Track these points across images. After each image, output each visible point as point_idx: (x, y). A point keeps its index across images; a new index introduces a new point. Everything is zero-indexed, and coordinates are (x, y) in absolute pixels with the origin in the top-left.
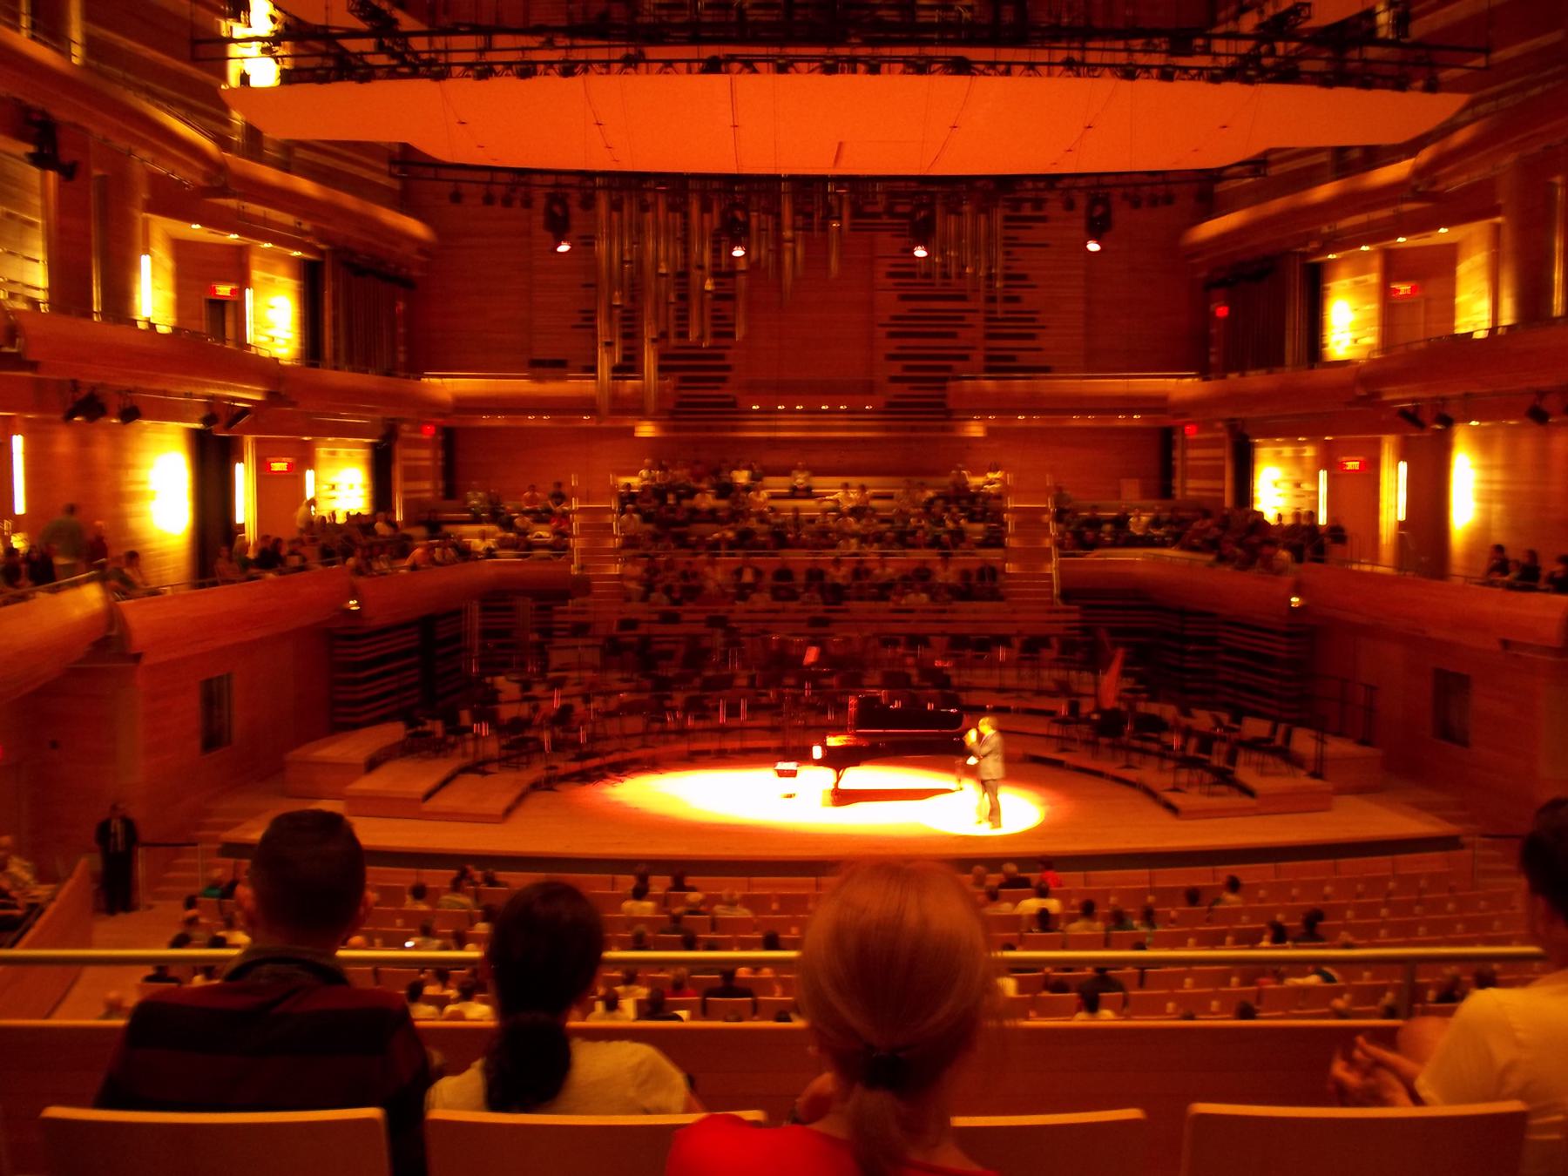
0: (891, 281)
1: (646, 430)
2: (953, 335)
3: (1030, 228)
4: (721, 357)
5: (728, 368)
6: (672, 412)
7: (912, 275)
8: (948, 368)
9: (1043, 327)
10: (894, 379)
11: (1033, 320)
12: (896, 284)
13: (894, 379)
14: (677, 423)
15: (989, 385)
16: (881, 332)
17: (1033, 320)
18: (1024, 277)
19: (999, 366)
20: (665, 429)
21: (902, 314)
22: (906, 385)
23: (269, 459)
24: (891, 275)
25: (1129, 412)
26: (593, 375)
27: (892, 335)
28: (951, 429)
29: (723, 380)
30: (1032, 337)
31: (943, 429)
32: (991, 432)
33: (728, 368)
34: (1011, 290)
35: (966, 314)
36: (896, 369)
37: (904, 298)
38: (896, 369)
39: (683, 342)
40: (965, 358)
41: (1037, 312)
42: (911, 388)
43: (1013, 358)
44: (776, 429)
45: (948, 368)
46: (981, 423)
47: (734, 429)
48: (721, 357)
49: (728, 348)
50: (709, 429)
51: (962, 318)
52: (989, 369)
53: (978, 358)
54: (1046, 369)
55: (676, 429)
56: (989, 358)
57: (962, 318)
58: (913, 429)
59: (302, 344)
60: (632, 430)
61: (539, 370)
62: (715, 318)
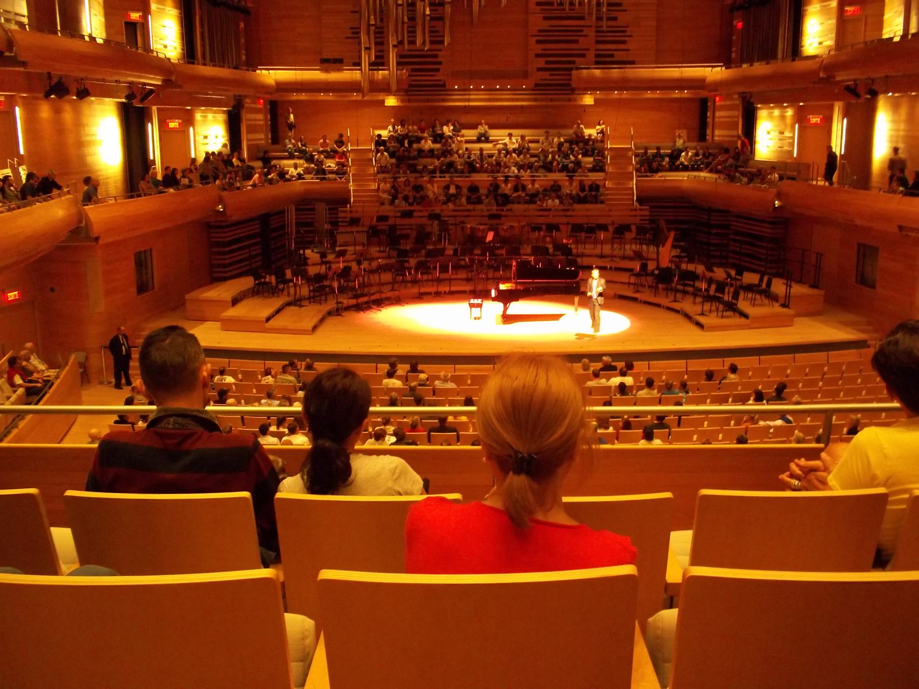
0: (539, 7)
1: (391, 101)
2: (576, 42)
4: (436, 56)
5: (440, 63)
6: (406, 90)
8: (573, 62)
10: (539, 69)
11: (625, 32)
12: (542, 10)
13: (539, 69)
15: (597, 72)
17: (625, 32)
18: (619, 5)
19: (603, 61)
20: (402, 101)
21: (545, 28)
22: (548, 73)
23: (167, 121)
25: (681, 88)
26: (359, 68)
27: (538, 42)
28: (575, 100)
29: (438, 70)
30: (624, 42)
31: (570, 100)
32: (596, 100)
33: (440, 63)
34: (612, 13)
35: (537, 34)
36: (541, 62)
37: (545, 18)
38: (541, 62)
39: (412, 47)
40: (583, 56)
41: (627, 27)
42: (550, 75)
43: (612, 56)
44: (469, 100)
45: (573, 62)
46: (593, 96)
47: (444, 100)
48: (436, 56)
49: (440, 50)
50: (428, 101)
52: (597, 63)
53: (591, 55)
54: (633, 63)
55: (409, 101)
56: (597, 56)
57: (582, 31)
58: (551, 100)
59: (183, 50)
60: (383, 101)
61: (326, 65)
62: (431, 32)
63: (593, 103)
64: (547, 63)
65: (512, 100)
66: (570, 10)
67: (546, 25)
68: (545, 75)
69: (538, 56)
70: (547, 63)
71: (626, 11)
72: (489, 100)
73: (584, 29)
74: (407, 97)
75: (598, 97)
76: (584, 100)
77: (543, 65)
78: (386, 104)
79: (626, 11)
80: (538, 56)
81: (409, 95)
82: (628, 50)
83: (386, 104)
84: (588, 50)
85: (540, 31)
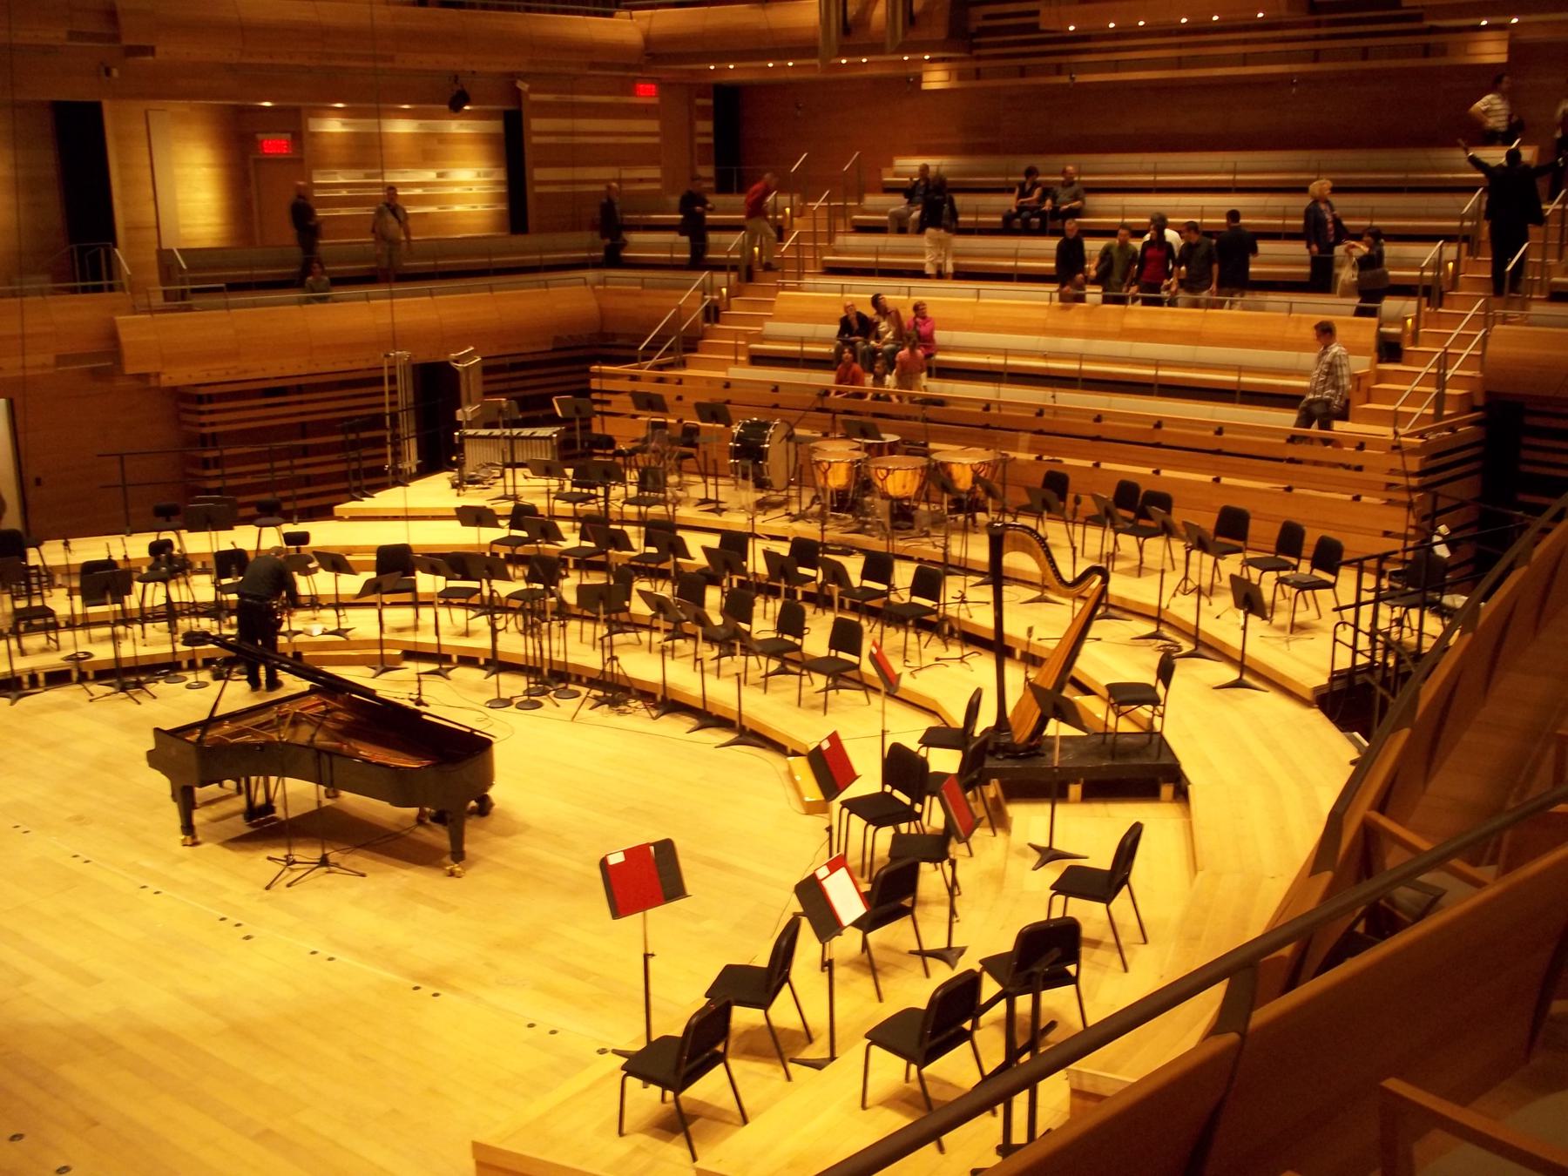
1: (936, 79)
14: (982, 64)
28: (1443, 51)
31: (1427, 51)
32: (1515, 49)
44: (1117, 66)
46: (1505, 35)
55: (978, 74)
58: (1365, 54)
60: (919, 79)
63: (1503, 59)
65: (1245, 60)
72: (1179, 63)
75: (1526, 36)
76: (1473, 49)
78: (925, 86)
81: (979, 58)
83: (925, 86)
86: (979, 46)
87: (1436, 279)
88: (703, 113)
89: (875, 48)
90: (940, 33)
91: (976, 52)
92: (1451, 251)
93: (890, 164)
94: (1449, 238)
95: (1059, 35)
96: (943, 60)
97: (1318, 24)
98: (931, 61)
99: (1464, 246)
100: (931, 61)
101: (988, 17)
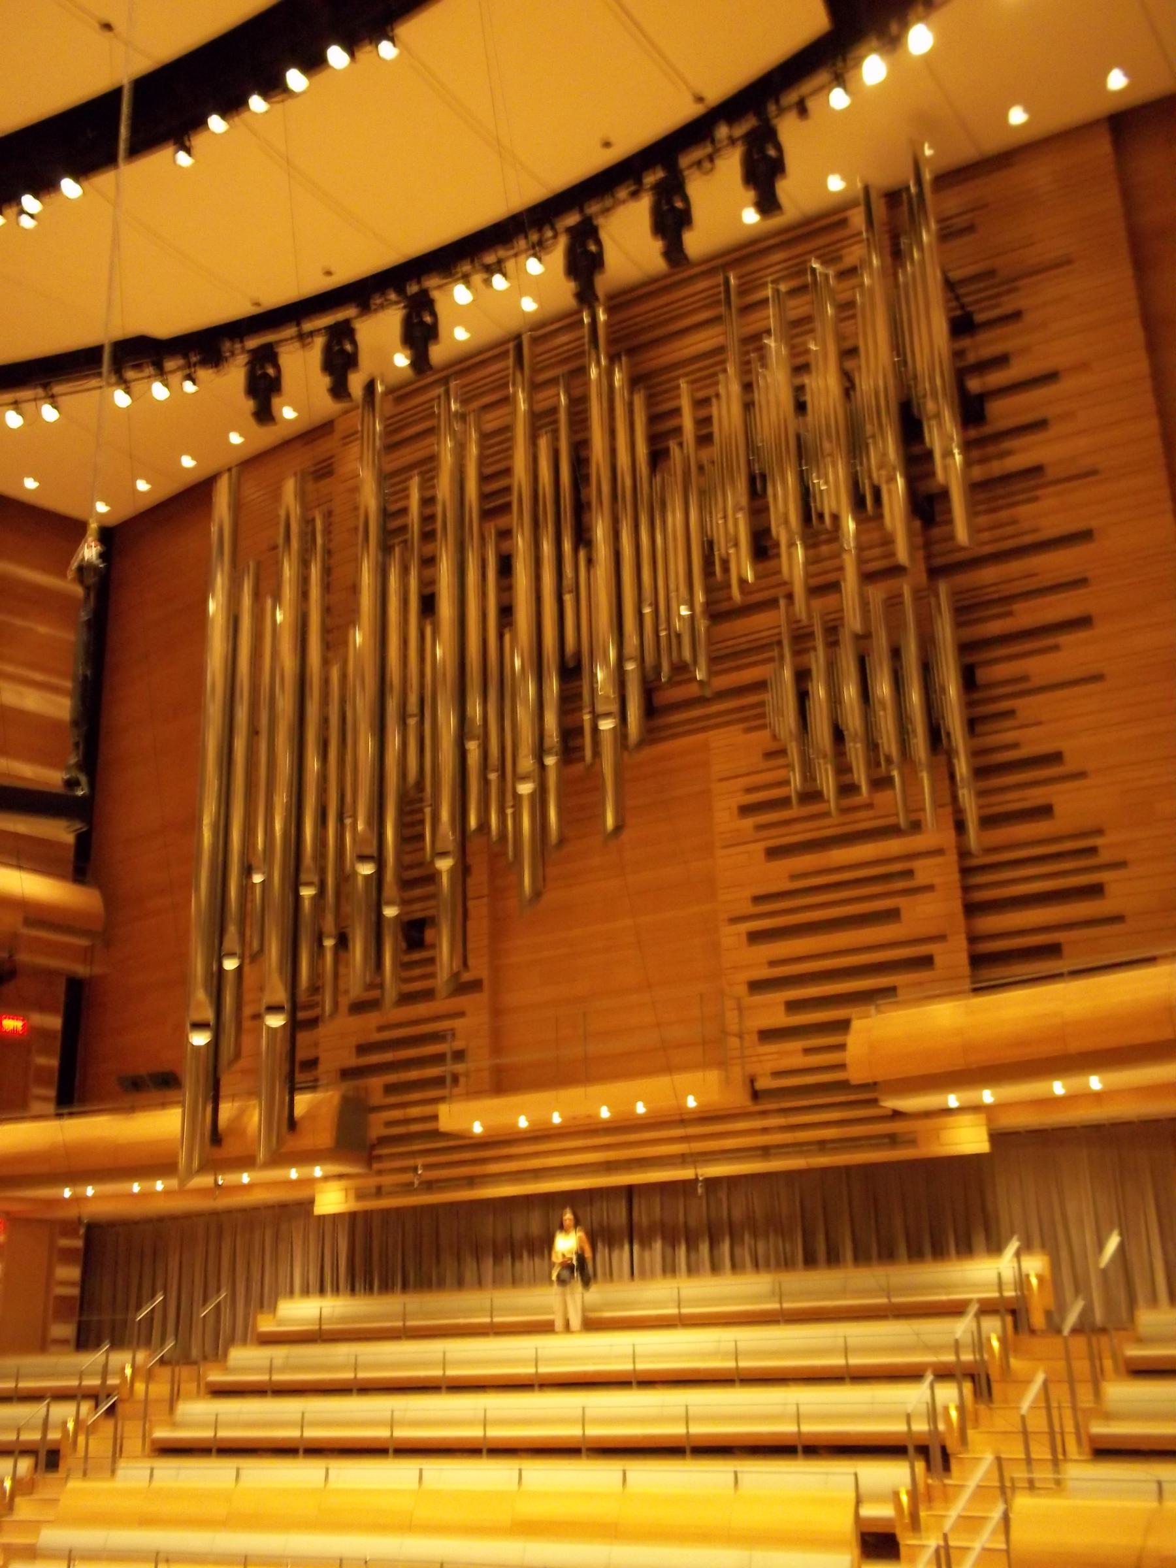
0: (749, 822)
2: (893, 915)
3: (1055, 648)
5: (459, 1055)
7: (784, 802)
9: (1121, 865)
10: (768, 1035)
12: (760, 827)
13: (768, 1035)
14: (387, 1180)
16: (732, 936)
17: (1093, 851)
18: (1055, 758)
20: (360, 1195)
24: (746, 810)
27: (755, 937)
28: (912, 1142)
30: (1095, 891)
31: (893, 1140)
33: (459, 1055)
37: (773, 853)
40: (926, 962)
41: (1099, 832)
42: (807, 1051)
47: (471, 1181)
49: (461, 1014)
51: (909, 873)
55: (379, 1192)
57: (909, 873)
60: (311, 1202)
64: (793, 1006)
66: (844, 811)
67: (778, 876)
68: (791, 1054)
69: (756, 986)
70: (793, 1006)
71: (1081, 775)
72: (609, 1167)
73: (917, 865)
74: (373, 1181)
77: (781, 1019)
79: (1081, 775)
80: (756, 986)
81: (380, 1172)
82: (1118, 919)
84: (941, 938)
85: (757, 899)
86: (380, 1158)
87: (934, 1432)
88: (67, 1256)
89: (247, 1162)
90: (324, 1137)
91: (376, 1166)
92: (948, 1394)
93: (273, 1308)
94: (944, 1374)
95: (467, 1141)
96: (340, 1177)
97: (764, 1113)
98: (326, 1178)
99: (968, 1387)
100: (326, 1178)
101: (390, 1124)
